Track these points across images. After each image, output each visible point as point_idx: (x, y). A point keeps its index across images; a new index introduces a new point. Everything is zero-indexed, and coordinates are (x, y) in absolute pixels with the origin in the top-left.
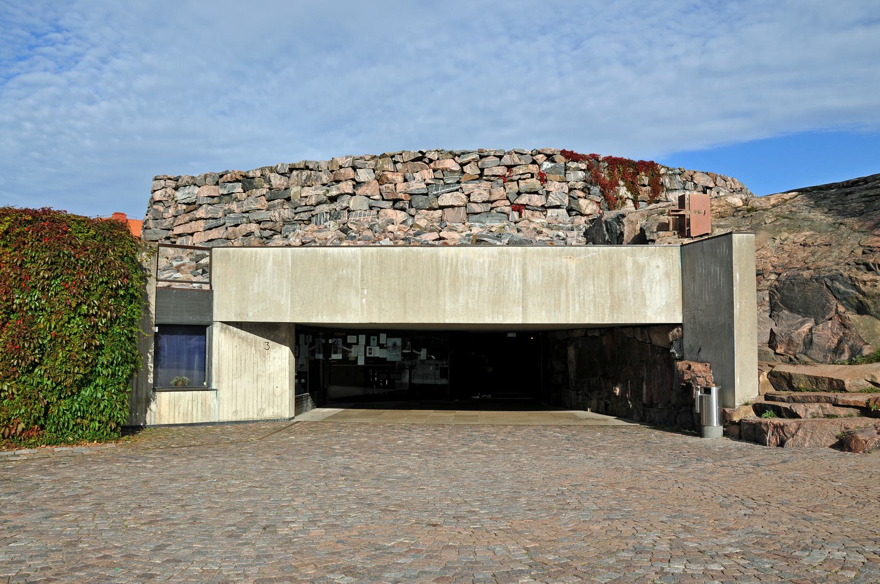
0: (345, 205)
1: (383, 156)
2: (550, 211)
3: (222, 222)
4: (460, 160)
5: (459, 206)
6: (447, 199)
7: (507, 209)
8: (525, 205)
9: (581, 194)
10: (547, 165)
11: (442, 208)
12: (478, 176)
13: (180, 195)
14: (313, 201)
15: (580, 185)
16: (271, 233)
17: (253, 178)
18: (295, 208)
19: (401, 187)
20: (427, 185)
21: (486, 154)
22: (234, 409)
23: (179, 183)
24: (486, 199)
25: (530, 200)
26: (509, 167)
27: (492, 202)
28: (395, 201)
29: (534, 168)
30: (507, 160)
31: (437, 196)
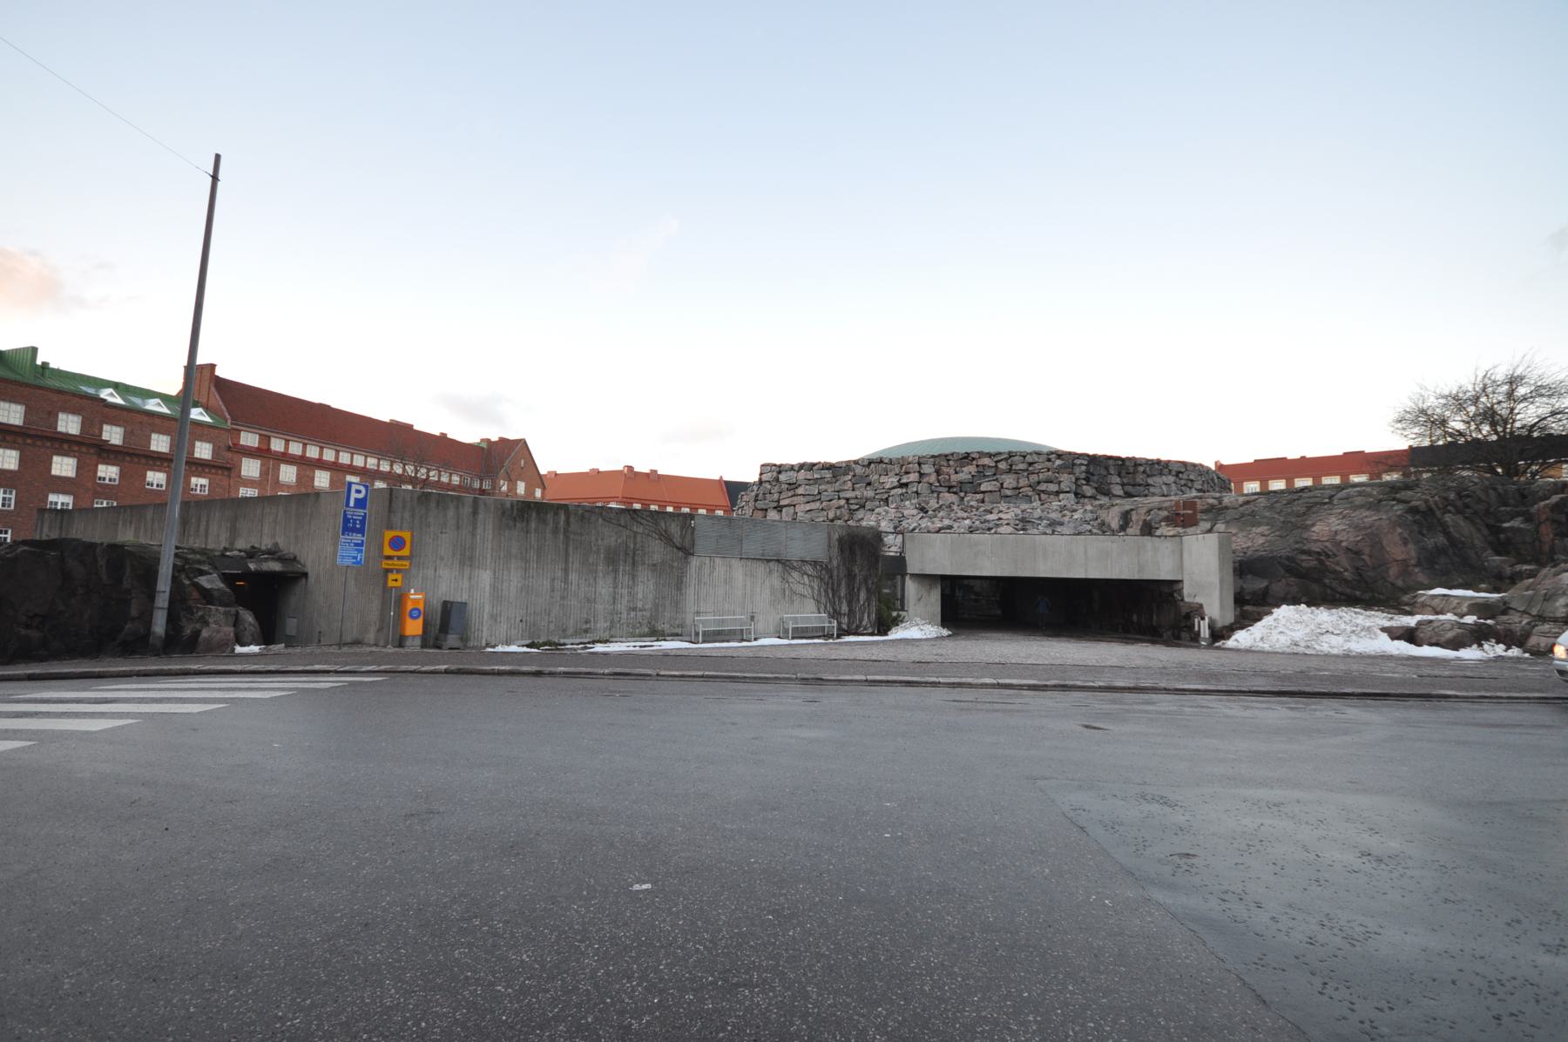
10: (1058, 462)
13: (782, 477)
19: (954, 477)
26: (1030, 464)
30: (1029, 459)
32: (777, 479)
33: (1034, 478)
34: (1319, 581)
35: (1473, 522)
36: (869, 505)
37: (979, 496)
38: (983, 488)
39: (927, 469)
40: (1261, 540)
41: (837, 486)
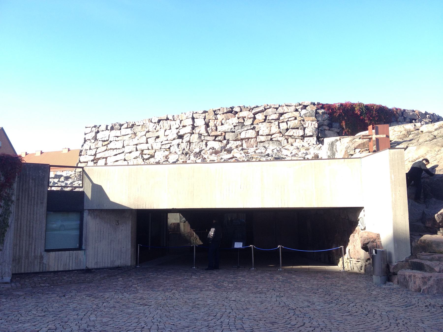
4: (254, 111)
5: (252, 138)
7: (280, 139)
8: (291, 136)
9: (327, 128)
11: (242, 140)
12: (263, 120)
13: (99, 136)
14: (170, 137)
15: (326, 122)
16: (149, 156)
18: (162, 142)
19: (219, 128)
20: (235, 126)
21: (268, 107)
22: (96, 261)
24: (268, 133)
25: (294, 133)
27: (271, 135)
28: (216, 136)
29: (296, 114)
30: (280, 110)
32: (95, 139)
33: (283, 126)
37: (239, 143)
38: (243, 136)
39: (200, 122)
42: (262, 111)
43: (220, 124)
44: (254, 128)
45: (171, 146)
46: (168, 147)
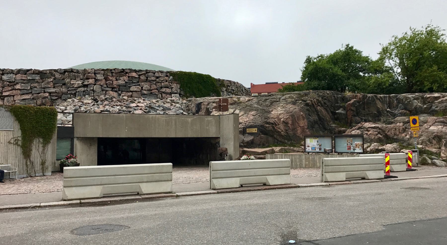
0: (92, 88)
1: (107, 70)
2: (173, 95)
3: (30, 91)
5: (138, 91)
6: (133, 88)
7: (157, 93)
8: (163, 92)
13: (5, 77)
17: (46, 73)
19: (115, 82)
20: (126, 82)
23: (4, 72)
26: (157, 77)
27: (151, 90)
29: (167, 78)
30: (157, 75)
31: (130, 87)
34: (272, 136)
35: (326, 110)
36: (64, 97)
40: (252, 117)
41: (43, 85)
42: (144, 74)
43: (115, 80)
44: (139, 85)
45: (76, 92)
46: (73, 93)
